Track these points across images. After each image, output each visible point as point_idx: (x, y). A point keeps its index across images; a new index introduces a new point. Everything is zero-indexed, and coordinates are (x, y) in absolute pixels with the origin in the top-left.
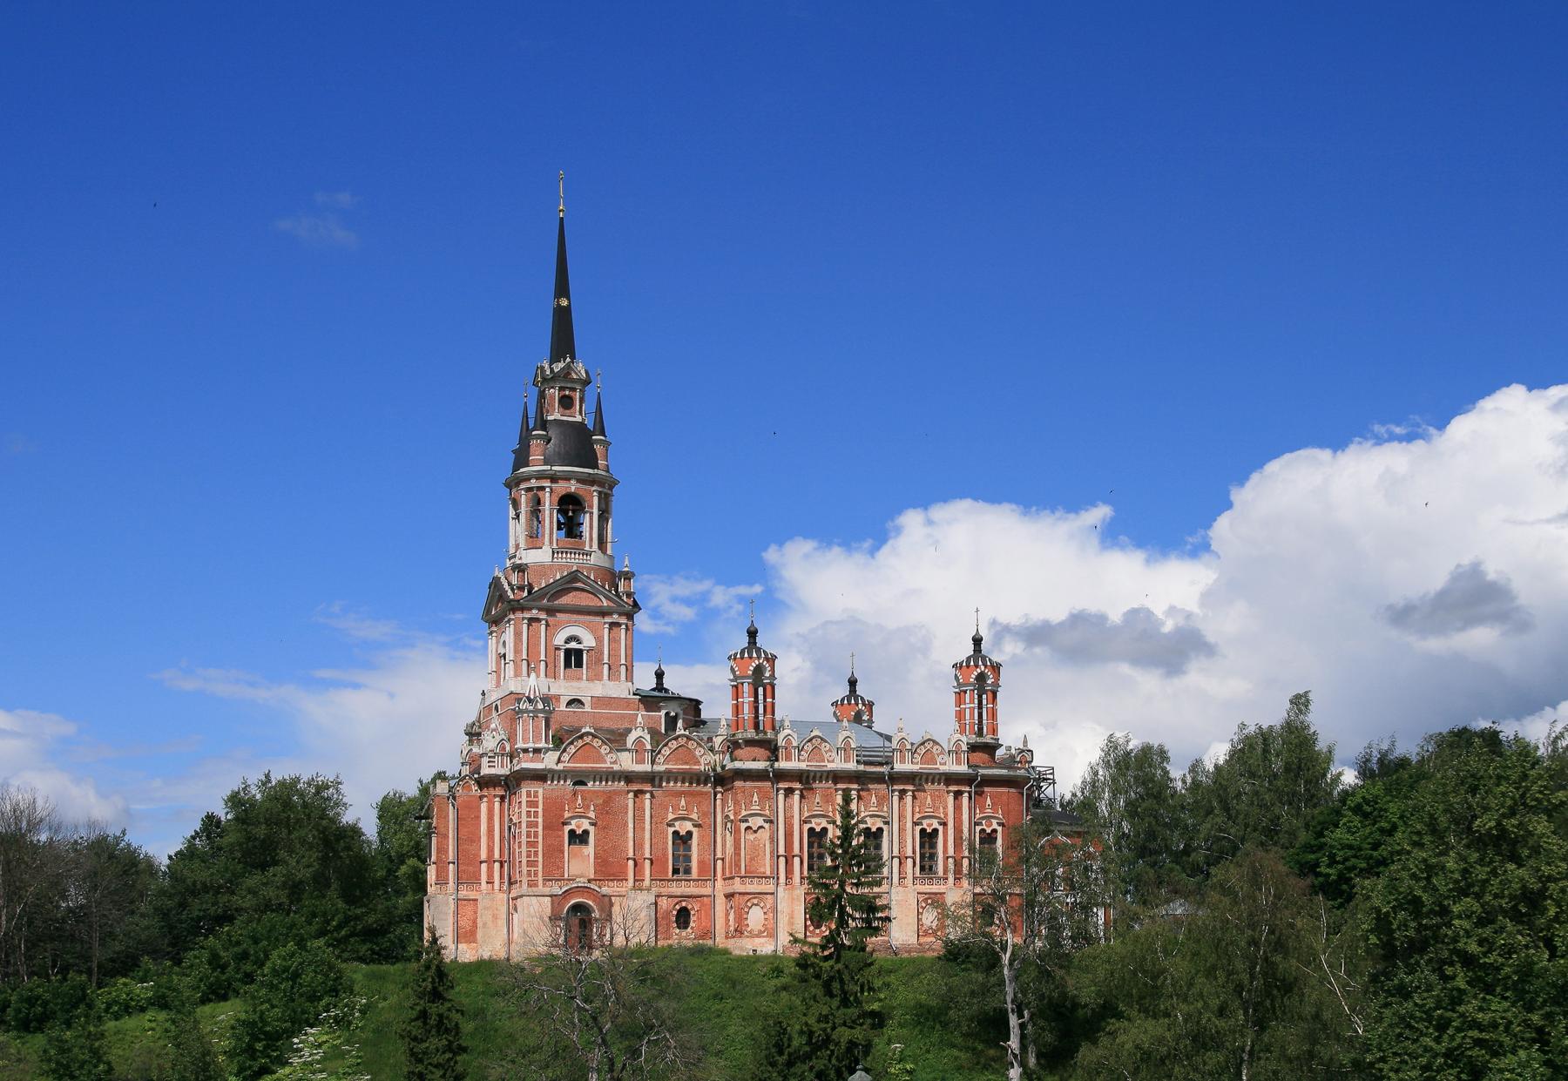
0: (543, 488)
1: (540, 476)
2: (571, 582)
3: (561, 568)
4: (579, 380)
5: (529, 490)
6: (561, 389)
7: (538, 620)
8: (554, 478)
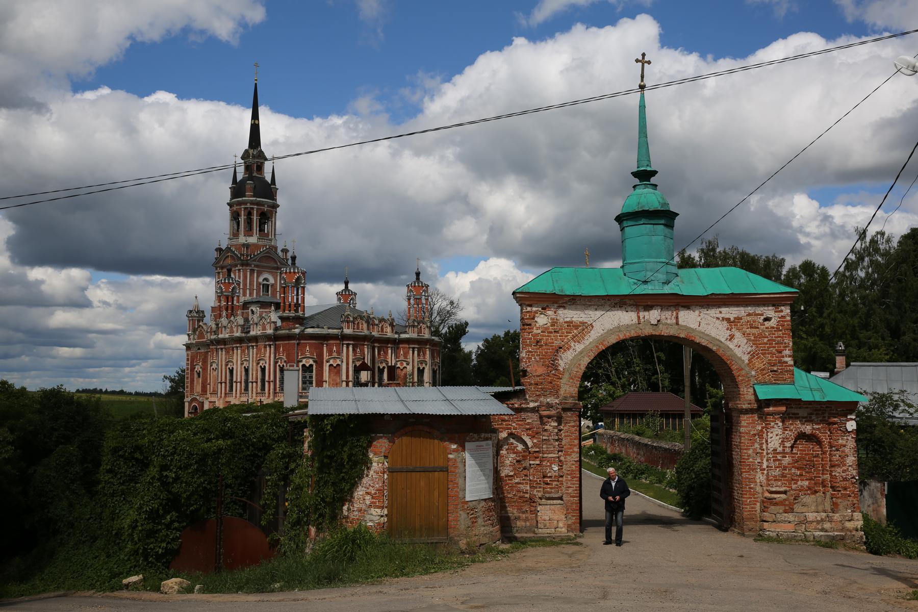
1: (252, 203)
3: (264, 246)
5: (245, 208)
8: (258, 204)
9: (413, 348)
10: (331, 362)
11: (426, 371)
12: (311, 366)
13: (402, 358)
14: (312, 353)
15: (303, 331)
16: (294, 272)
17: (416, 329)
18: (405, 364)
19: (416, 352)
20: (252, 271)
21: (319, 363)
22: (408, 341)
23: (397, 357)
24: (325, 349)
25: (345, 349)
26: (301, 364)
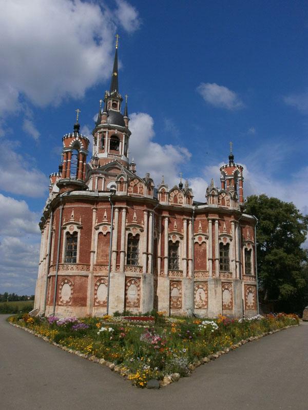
0: (105, 132)
1: (104, 127)
2: (113, 166)
3: (111, 160)
4: (119, 98)
5: (100, 133)
6: (113, 101)
7: (102, 178)
8: (110, 128)
9: (213, 221)
10: (101, 230)
11: (231, 247)
12: (76, 233)
13: (200, 231)
14: (76, 218)
15: (69, 192)
16: (71, 137)
17: (216, 199)
18: (203, 237)
19: (216, 225)
20: (99, 178)
21: (86, 230)
22: (207, 212)
23: (194, 230)
24: (94, 215)
25: (116, 214)
26: (65, 231)
